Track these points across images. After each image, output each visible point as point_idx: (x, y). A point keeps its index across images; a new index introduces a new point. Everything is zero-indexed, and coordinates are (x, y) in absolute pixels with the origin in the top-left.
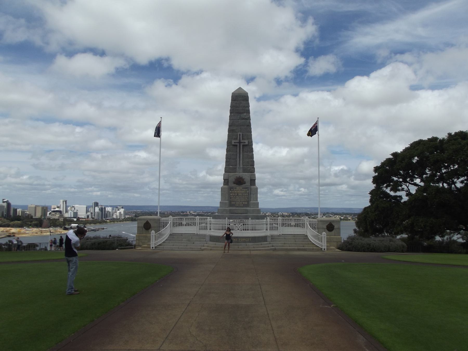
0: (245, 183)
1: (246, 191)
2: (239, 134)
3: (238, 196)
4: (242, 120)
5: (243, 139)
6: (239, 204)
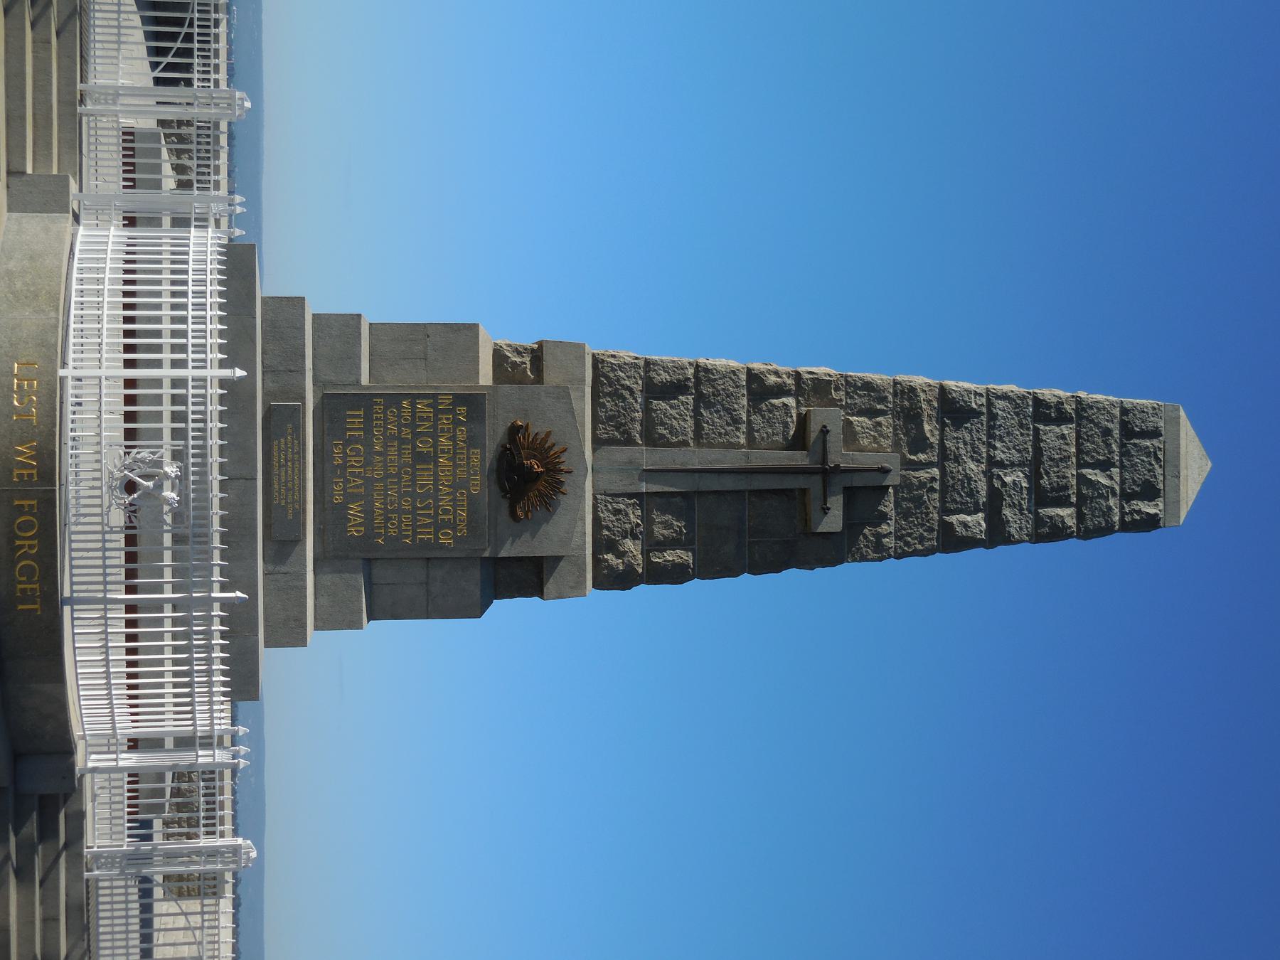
2: (891, 461)
3: (407, 457)
6: (343, 467)
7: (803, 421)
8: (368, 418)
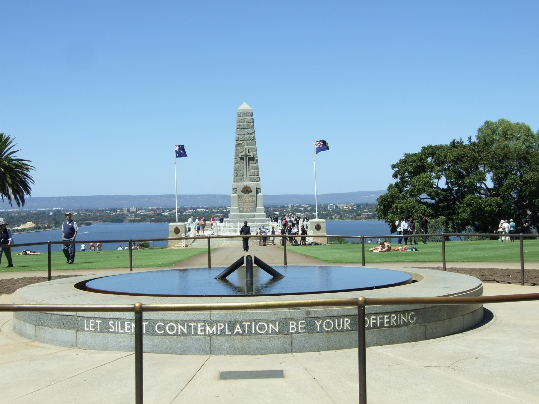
0: (252, 192)
1: (253, 198)
2: (245, 147)
4: (247, 134)
5: (249, 152)
7: (240, 158)
8: (241, 207)
